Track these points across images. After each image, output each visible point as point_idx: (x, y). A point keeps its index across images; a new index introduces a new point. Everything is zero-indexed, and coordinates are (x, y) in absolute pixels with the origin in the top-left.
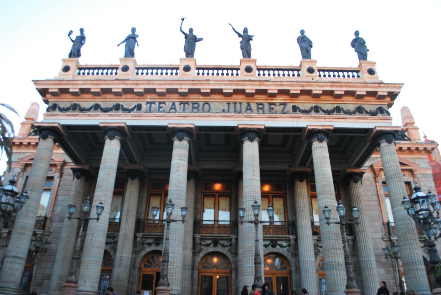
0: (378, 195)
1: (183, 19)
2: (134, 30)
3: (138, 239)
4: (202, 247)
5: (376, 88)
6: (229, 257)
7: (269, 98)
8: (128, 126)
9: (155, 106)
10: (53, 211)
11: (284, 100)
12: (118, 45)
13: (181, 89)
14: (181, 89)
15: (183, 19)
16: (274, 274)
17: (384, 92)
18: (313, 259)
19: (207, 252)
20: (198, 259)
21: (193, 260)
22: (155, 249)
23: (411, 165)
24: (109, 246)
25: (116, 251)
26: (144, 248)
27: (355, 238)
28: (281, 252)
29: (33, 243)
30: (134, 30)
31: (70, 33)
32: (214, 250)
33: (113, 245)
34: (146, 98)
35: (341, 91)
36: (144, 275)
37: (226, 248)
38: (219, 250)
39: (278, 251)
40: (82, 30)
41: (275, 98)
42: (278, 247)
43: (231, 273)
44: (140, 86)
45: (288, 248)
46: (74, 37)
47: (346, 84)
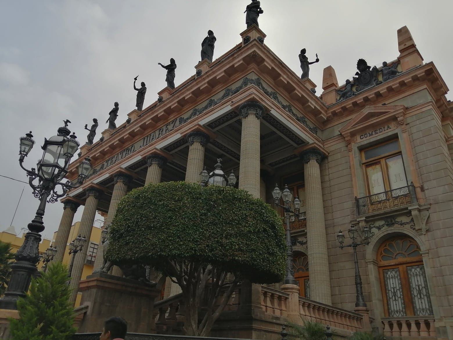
1: (136, 79)
2: (116, 104)
5: (232, 61)
7: (165, 121)
8: (97, 184)
9: (109, 162)
11: (173, 117)
12: (107, 121)
13: (115, 142)
14: (115, 142)
15: (136, 79)
17: (239, 61)
23: (392, 111)
30: (116, 104)
31: (86, 125)
34: (106, 158)
35: (204, 84)
40: (95, 121)
41: (169, 119)
44: (98, 151)
46: (89, 127)
47: (206, 75)
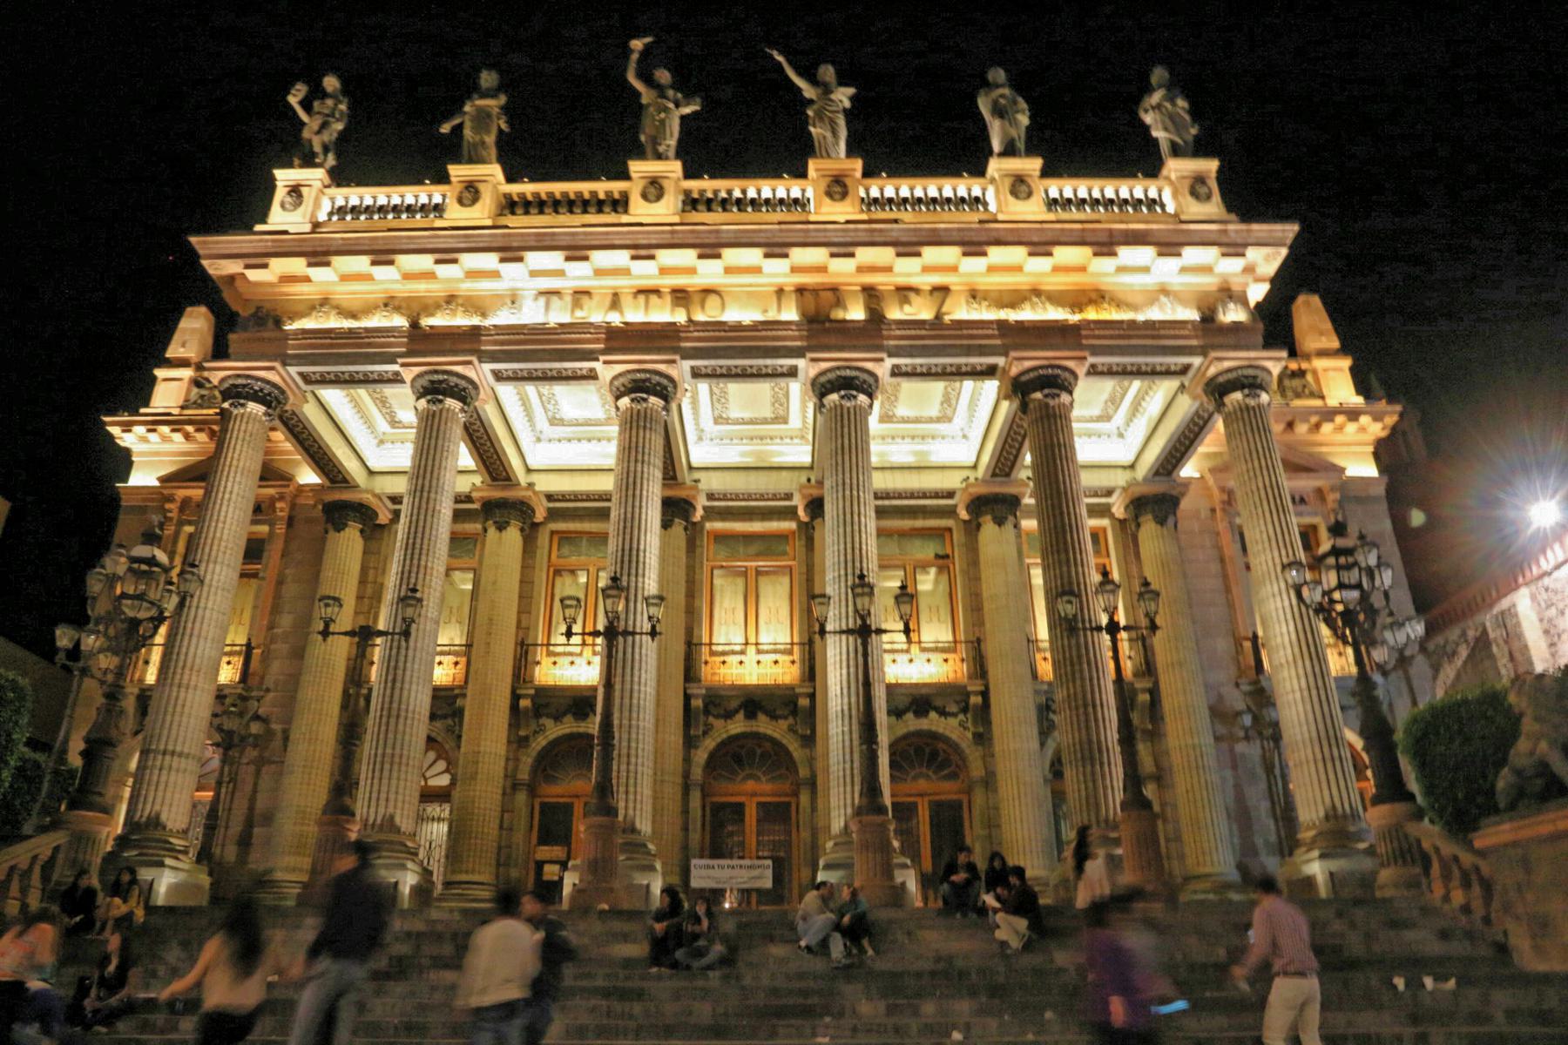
0: (1222, 560)
3: (525, 703)
4: (711, 719)
6: (791, 748)
10: (271, 627)
16: (921, 795)
18: (1035, 745)
19: (725, 736)
20: (701, 756)
21: (687, 760)
22: (575, 730)
24: (438, 724)
25: (460, 737)
26: (541, 730)
27: (1156, 683)
28: (941, 730)
29: (217, 721)
32: (748, 730)
33: (450, 721)
36: (543, 805)
37: (781, 722)
38: (762, 730)
39: (934, 728)
42: (933, 715)
43: (796, 794)
45: (961, 717)
